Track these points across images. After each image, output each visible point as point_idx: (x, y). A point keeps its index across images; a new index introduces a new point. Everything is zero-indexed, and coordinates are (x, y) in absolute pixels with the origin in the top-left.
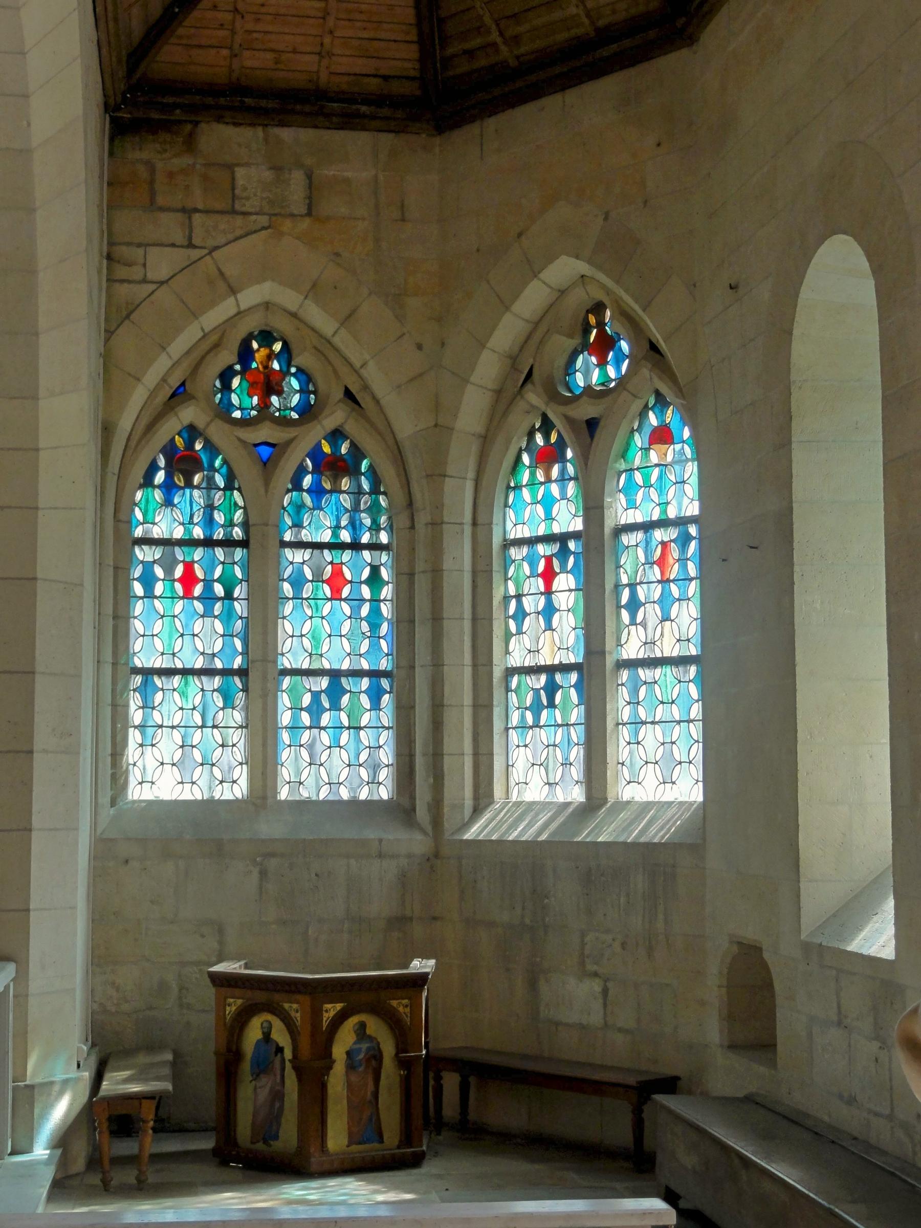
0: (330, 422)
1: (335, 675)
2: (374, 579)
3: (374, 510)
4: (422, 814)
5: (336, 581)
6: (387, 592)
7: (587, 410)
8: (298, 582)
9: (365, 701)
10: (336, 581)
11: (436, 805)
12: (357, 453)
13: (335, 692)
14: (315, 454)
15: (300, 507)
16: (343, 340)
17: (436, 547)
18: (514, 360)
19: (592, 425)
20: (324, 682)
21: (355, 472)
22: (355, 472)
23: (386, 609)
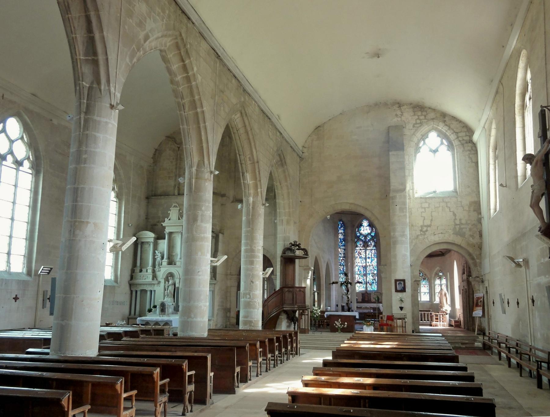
0: (424, 276)
1: (425, 293)
2: (427, 286)
3: (427, 282)
4: (431, 302)
5: (425, 286)
6: (428, 287)
7: (440, 277)
8: (422, 286)
9: (427, 294)
10: (425, 286)
11: (432, 301)
12: (426, 278)
13: (425, 294)
14: (423, 278)
15: (422, 282)
16: (425, 271)
17: (431, 285)
18: (435, 273)
19: (440, 277)
20: (424, 293)
21: (426, 279)
22: (425, 279)
23: (428, 288)
